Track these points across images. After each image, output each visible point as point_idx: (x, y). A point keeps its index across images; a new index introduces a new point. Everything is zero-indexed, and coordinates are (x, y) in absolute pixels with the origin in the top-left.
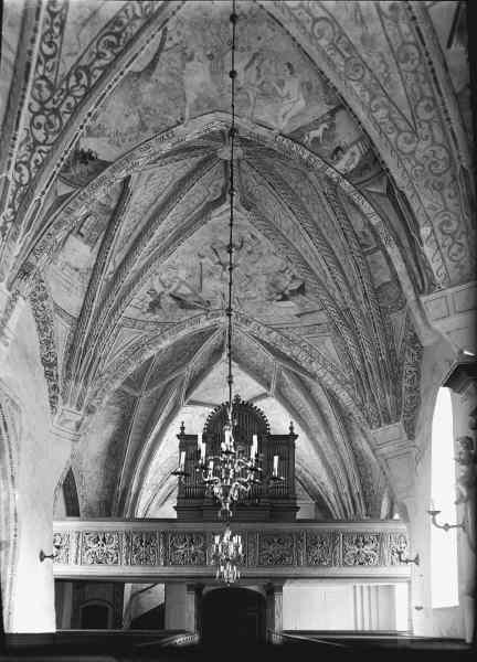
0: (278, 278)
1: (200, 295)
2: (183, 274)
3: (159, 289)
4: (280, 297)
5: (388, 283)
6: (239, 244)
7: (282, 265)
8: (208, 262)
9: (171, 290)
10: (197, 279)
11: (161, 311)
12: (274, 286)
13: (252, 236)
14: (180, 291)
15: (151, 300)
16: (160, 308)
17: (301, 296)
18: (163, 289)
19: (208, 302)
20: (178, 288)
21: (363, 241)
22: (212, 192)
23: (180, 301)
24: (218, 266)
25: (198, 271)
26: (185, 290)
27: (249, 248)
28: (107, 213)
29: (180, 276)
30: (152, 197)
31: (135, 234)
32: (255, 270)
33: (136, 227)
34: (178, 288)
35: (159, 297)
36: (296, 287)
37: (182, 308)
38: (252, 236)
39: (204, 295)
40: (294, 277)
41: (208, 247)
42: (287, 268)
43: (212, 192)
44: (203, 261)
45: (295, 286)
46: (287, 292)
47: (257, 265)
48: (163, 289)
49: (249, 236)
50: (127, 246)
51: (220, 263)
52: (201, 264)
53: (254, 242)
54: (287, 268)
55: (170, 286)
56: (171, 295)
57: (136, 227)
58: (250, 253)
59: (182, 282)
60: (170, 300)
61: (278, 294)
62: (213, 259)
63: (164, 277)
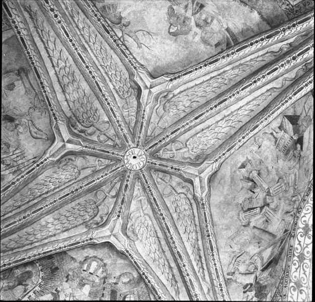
0: (281, 146)
1: (277, 238)
2: (253, 250)
3: (250, 280)
4: (299, 146)
5: (259, 13)
6: (250, 184)
7: (270, 140)
8: (257, 220)
9: (260, 268)
10: (266, 237)
11: (268, 289)
12: (288, 151)
13: (243, 166)
14: (265, 260)
15: (253, 293)
16: (266, 287)
17: (300, 122)
18: (253, 276)
19: (286, 231)
20: (262, 259)
21: (224, 46)
22: (184, 191)
23: (273, 262)
24: (264, 210)
25: (257, 232)
26: (267, 255)
27: (255, 174)
28: (138, 283)
29: (252, 253)
30: (153, 239)
31: (176, 271)
32: (274, 171)
33: (170, 268)
34: (262, 259)
35: (257, 283)
36: (291, 125)
37: (277, 264)
38: (243, 166)
39: (280, 235)
40: (281, 128)
41: (242, 215)
42: (272, 134)
43: (184, 191)
44: (252, 225)
45: (289, 126)
46: (295, 138)
47: (270, 168)
48: (253, 276)
49: (243, 170)
50: (180, 284)
51: (262, 208)
52: (254, 227)
53: (249, 167)
54: (272, 134)
55: (256, 268)
56: (263, 270)
57: (170, 268)
58: (259, 174)
59: (260, 253)
60: (266, 274)
61: (296, 149)
62: (256, 214)
63: (242, 269)
